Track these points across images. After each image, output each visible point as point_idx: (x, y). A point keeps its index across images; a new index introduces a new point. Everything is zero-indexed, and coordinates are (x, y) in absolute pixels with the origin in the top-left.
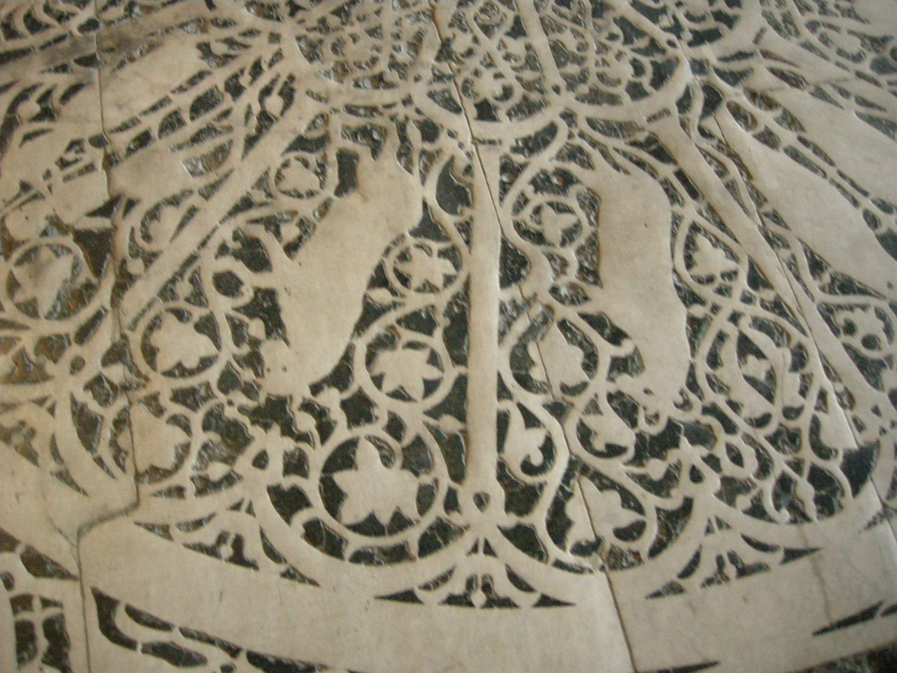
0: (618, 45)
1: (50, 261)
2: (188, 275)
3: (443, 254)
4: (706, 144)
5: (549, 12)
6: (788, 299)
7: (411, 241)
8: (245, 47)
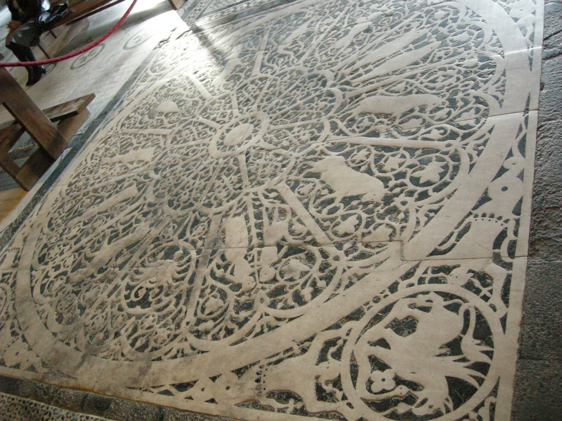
1: (289, 267)
2: (322, 222)
3: (358, 151)
6: (422, 71)
7: (349, 159)
8: (245, 202)
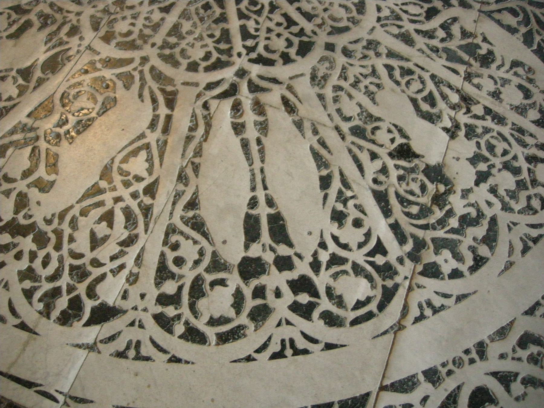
0: (209, 41)
4: (200, 112)
5: (192, 9)
